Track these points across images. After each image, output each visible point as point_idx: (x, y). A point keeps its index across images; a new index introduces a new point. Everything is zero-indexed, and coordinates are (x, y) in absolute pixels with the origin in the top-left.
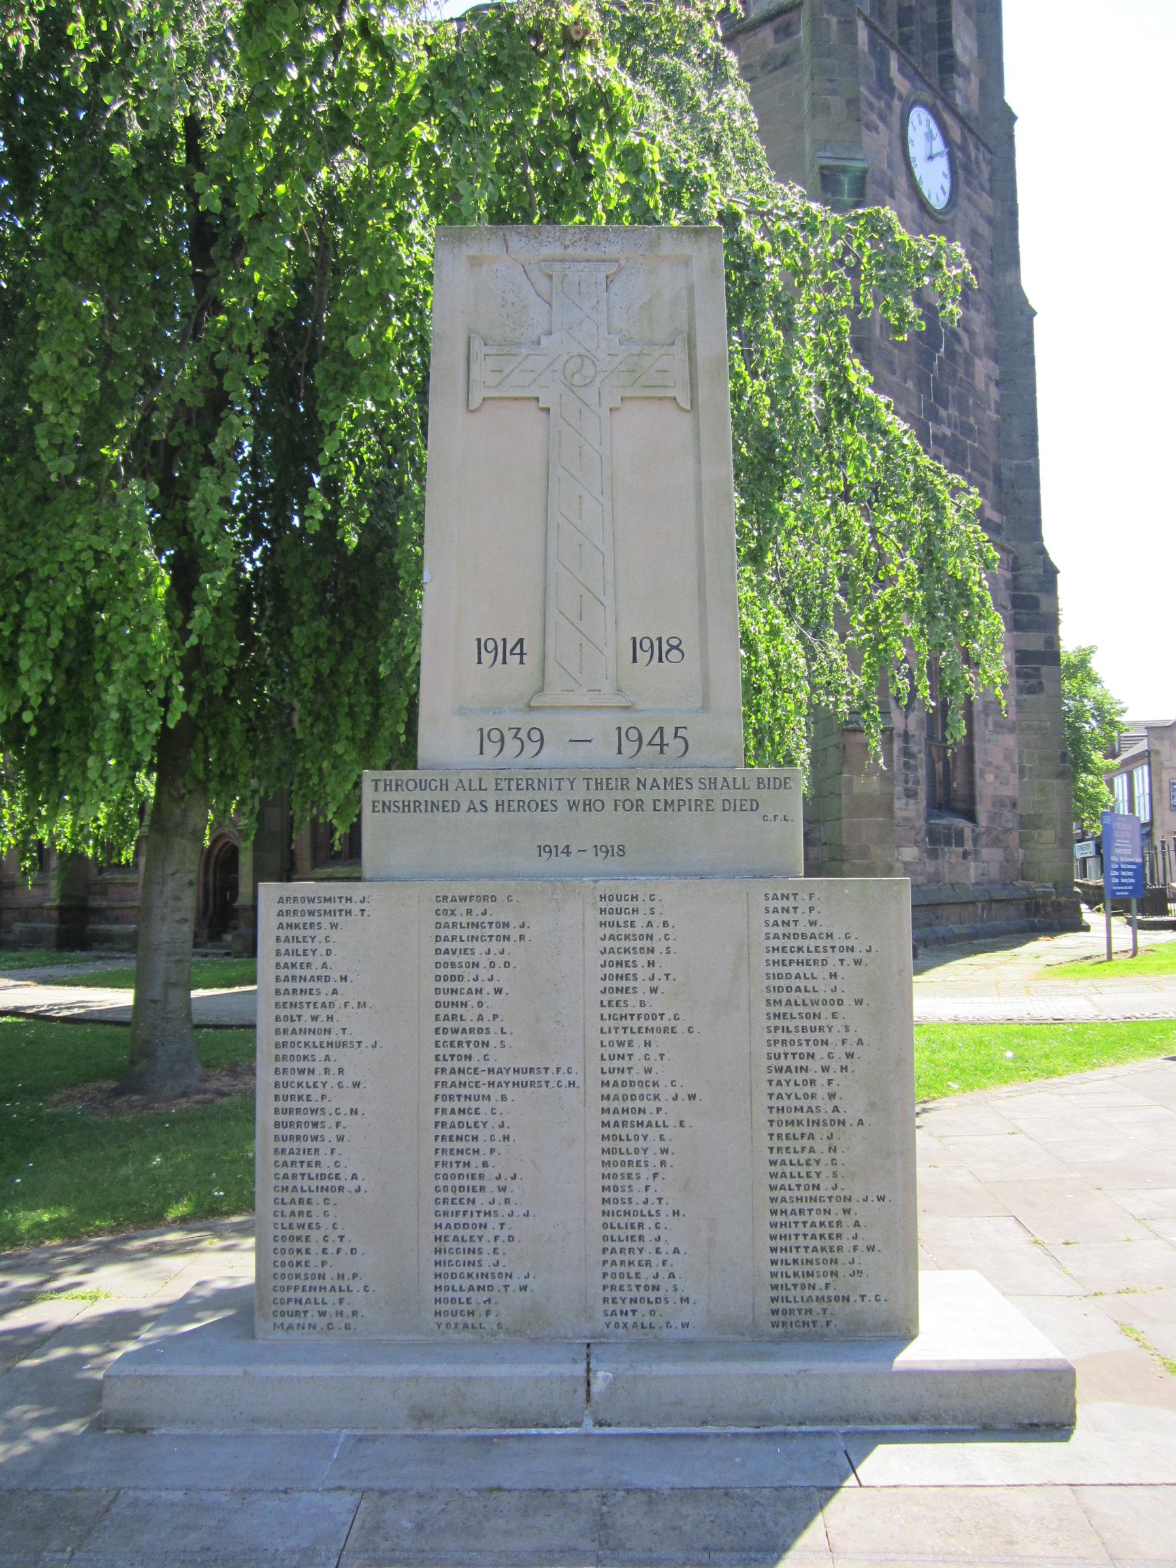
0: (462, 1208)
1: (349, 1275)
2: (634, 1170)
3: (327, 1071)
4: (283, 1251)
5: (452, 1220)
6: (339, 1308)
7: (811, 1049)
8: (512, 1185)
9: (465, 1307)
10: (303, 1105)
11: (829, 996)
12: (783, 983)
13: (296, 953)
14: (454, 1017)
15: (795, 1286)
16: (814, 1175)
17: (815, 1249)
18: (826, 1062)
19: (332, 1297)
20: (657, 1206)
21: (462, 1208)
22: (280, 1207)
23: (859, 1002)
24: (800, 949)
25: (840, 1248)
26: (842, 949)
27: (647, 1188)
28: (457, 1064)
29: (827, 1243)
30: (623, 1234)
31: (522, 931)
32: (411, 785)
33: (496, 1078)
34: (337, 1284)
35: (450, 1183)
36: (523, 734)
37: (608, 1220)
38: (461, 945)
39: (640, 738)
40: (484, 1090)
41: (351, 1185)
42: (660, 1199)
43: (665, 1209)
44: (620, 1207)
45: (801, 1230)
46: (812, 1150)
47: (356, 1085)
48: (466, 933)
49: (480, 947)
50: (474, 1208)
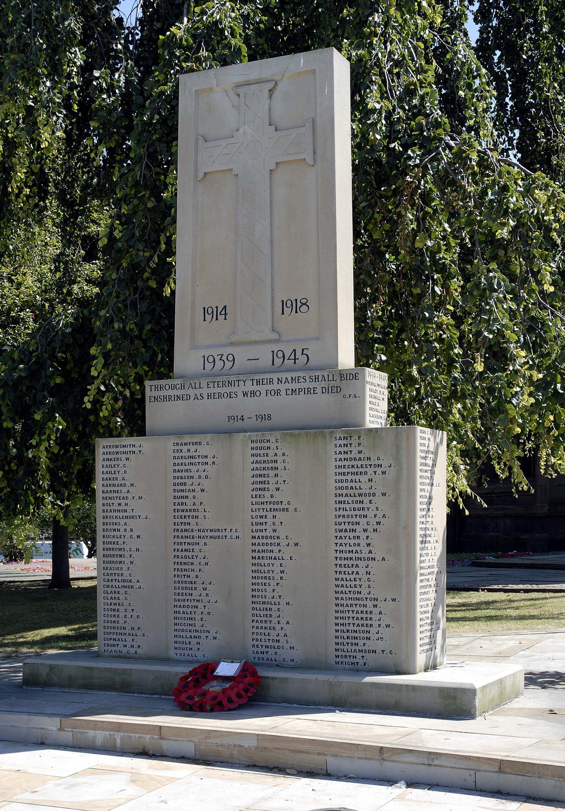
0: (186, 598)
1: (136, 628)
2: (267, 581)
3: (125, 530)
4: (108, 616)
5: (182, 604)
6: (132, 643)
7: (358, 520)
8: (209, 587)
9: (188, 646)
10: (115, 546)
11: (367, 491)
12: (344, 485)
13: (111, 473)
14: (182, 504)
15: (348, 643)
16: (358, 586)
17: (358, 625)
18: (366, 527)
19: (129, 638)
20: (278, 600)
21: (186, 598)
22: (106, 595)
23: (384, 494)
24: (353, 466)
25: (371, 625)
26: (375, 466)
27: (274, 590)
28: (184, 527)
29: (365, 622)
30: (262, 613)
31: (214, 460)
32: (167, 387)
33: (202, 534)
34: (131, 632)
35: (181, 585)
36: (224, 358)
37: (255, 606)
38: (186, 468)
39: (284, 356)
40: (196, 540)
41: (137, 585)
42: (280, 596)
43: (283, 602)
44: (260, 599)
45: (351, 615)
46: (357, 573)
47: (138, 537)
48: (187, 461)
49: (194, 468)
50: (192, 598)
